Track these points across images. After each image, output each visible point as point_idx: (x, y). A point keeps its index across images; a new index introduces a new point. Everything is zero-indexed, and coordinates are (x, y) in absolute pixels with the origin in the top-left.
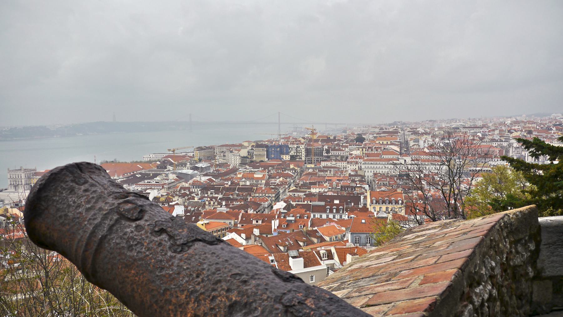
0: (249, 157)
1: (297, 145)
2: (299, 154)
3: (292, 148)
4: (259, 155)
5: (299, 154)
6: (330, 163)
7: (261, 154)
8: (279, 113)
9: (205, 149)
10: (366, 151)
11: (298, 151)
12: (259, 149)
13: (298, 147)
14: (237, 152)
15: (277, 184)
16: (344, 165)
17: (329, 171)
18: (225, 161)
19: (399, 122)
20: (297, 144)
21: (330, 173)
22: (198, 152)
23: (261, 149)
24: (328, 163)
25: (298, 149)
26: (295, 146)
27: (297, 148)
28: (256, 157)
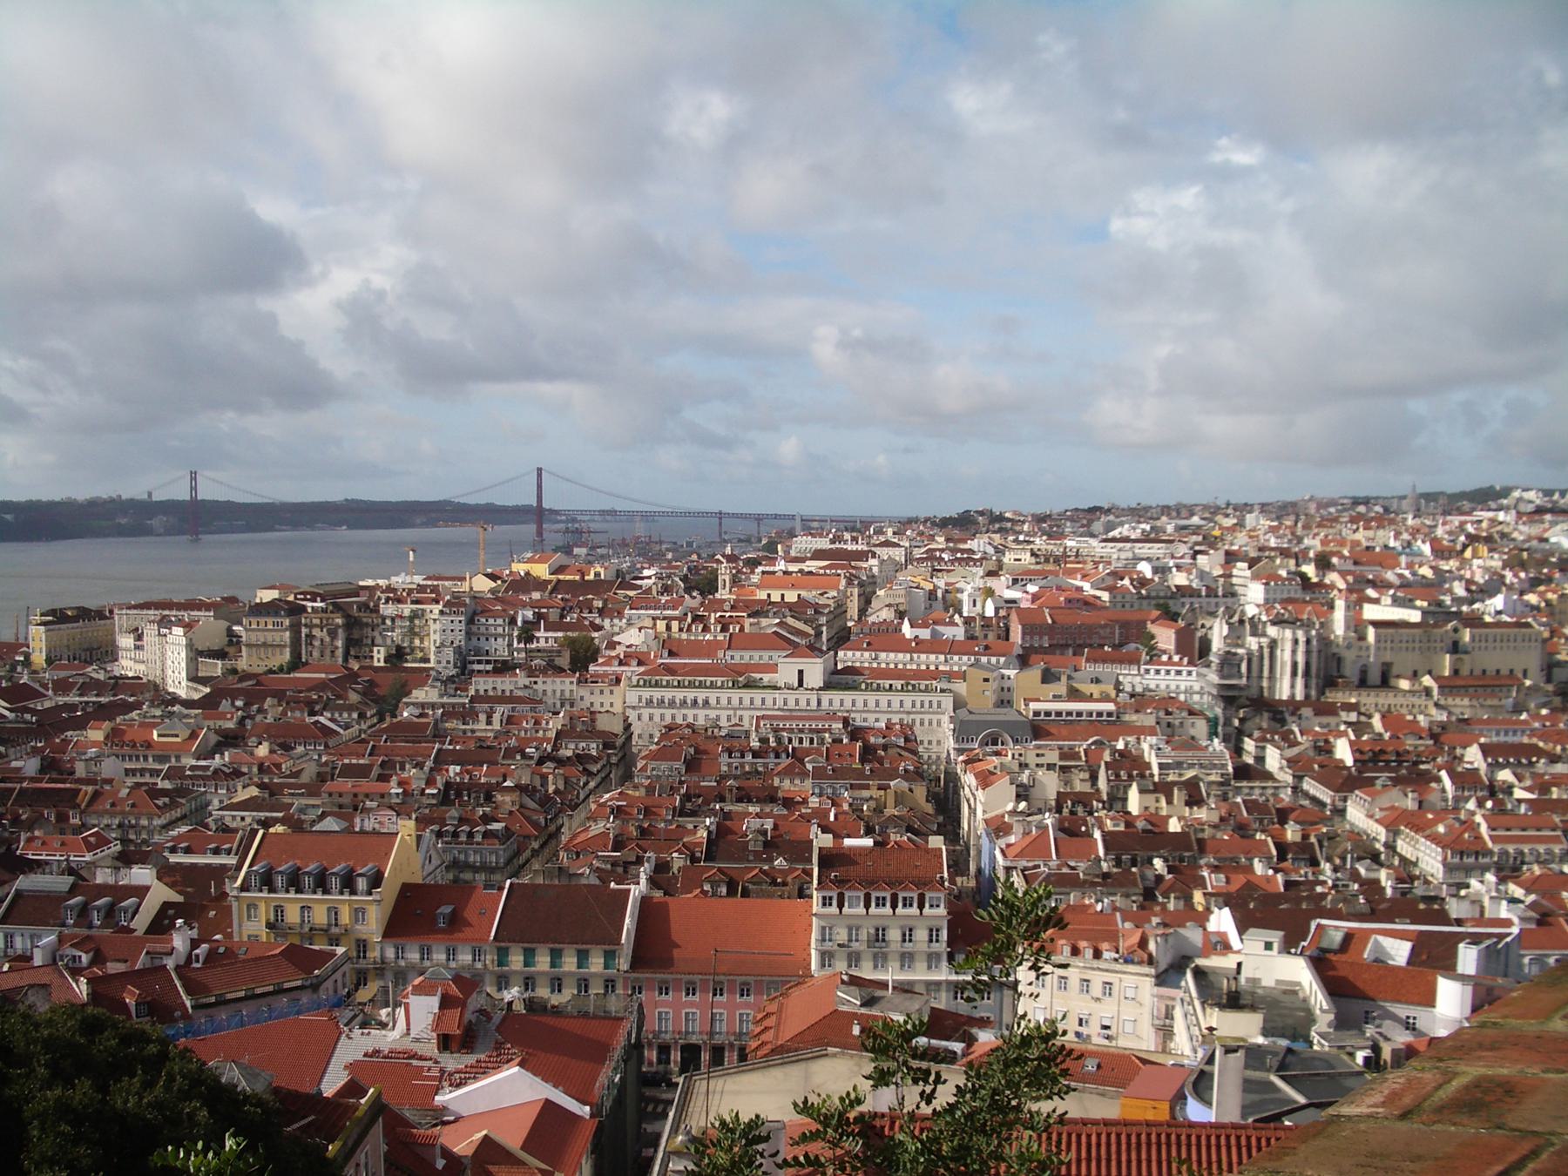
0: (231, 650)
1: (415, 607)
2: (422, 642)
3: (393, 620)
4: (265, 645)
5: (422, 642)
6: (507, 679)
7: (269, 640)
8: (540, 470)
9: (75, 619)
10: (681, 630)
11: (417, 630)
12: (262, 621)
13: (414, 615)
14: (178, 631)
15: (216, 771)
16: (562, 691)
17: (483, 717)
18: (142, 667)
19: (981, 513)
20: (413, 602)
21: (489, 723)
22: (42, 628)
23: (270, 620)
24: (499, 680)
25: (417, 622)
26: (407, 609)
27: (412, 618)
28: (250, 656)
